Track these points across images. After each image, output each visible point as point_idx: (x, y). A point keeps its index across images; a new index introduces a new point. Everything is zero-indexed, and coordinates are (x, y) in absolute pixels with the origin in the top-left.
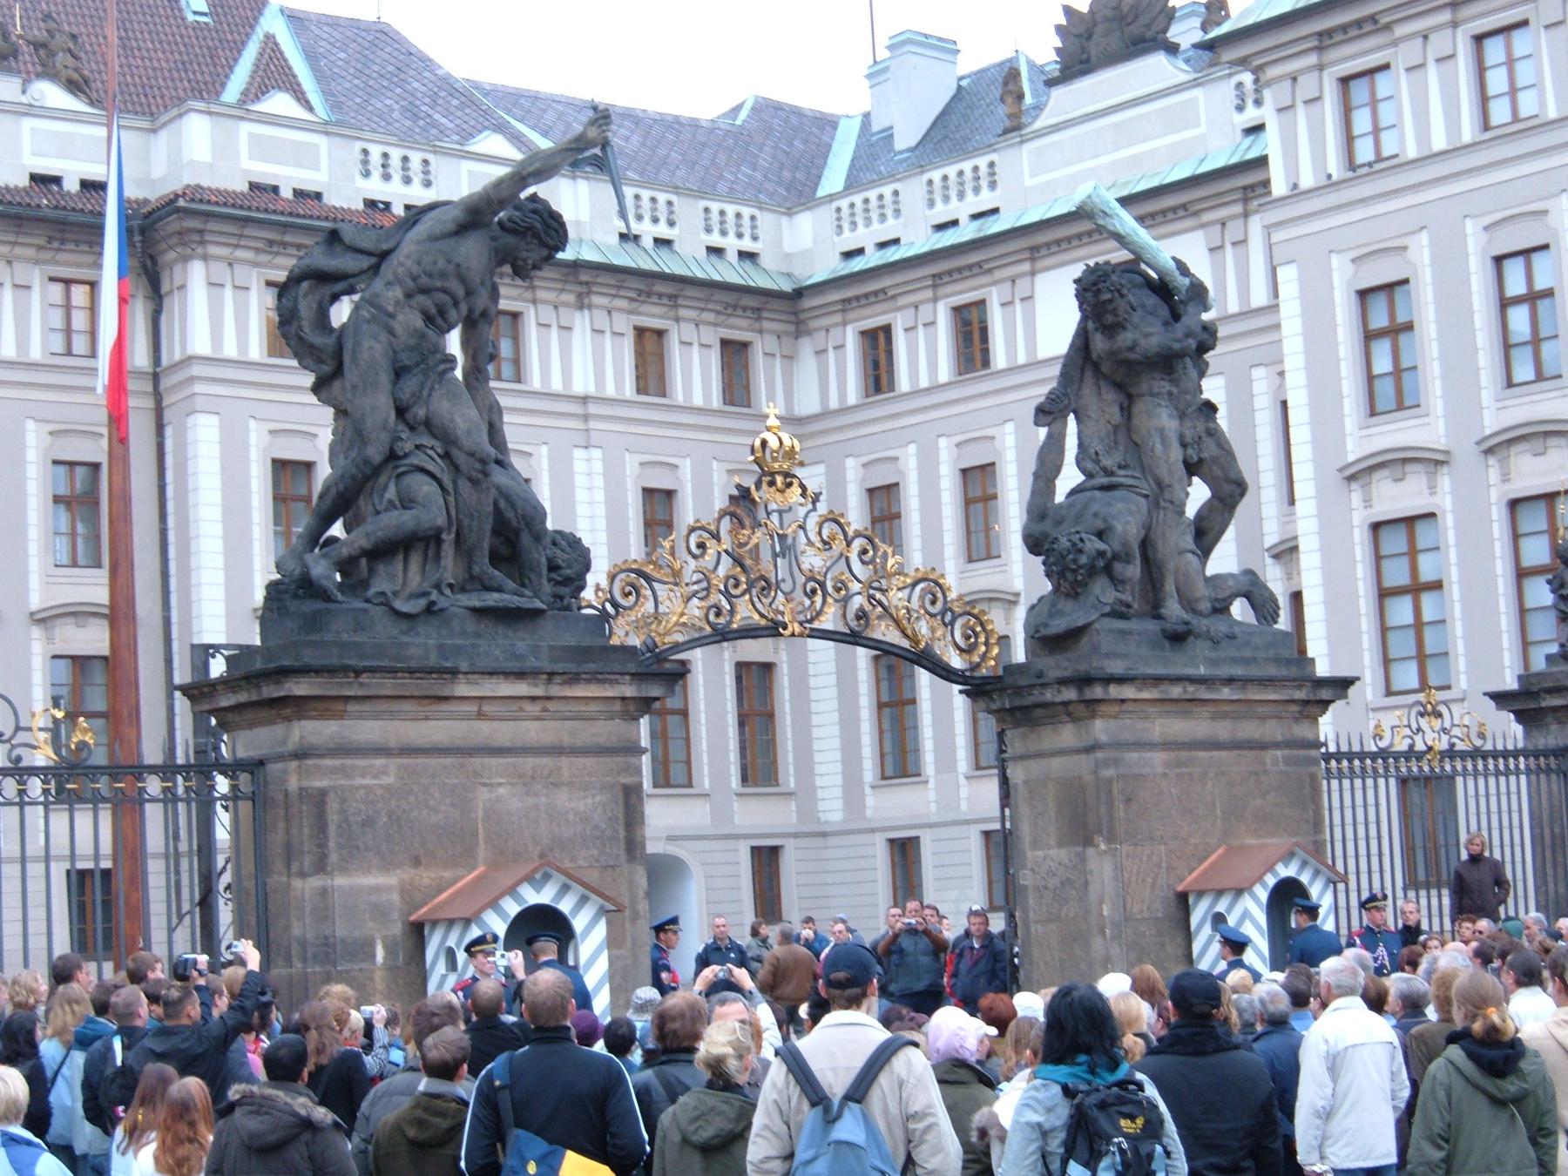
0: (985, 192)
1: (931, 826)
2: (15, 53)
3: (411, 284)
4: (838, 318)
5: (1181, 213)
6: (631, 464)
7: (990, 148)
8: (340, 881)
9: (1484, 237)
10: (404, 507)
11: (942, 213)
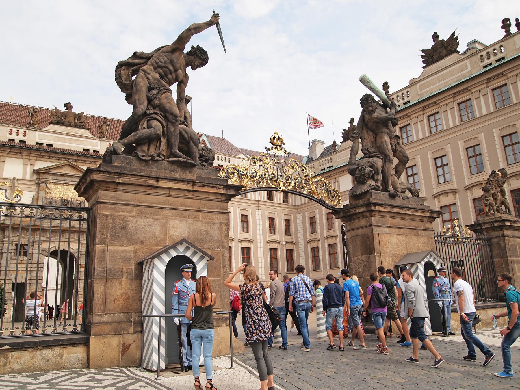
0: (330, 163)
1: (322, 279)
3: (156, 65)
7: (331, 155)
8: (110, 247)
9: (432, 155)
10: (148, 129)
11: (322, 167)
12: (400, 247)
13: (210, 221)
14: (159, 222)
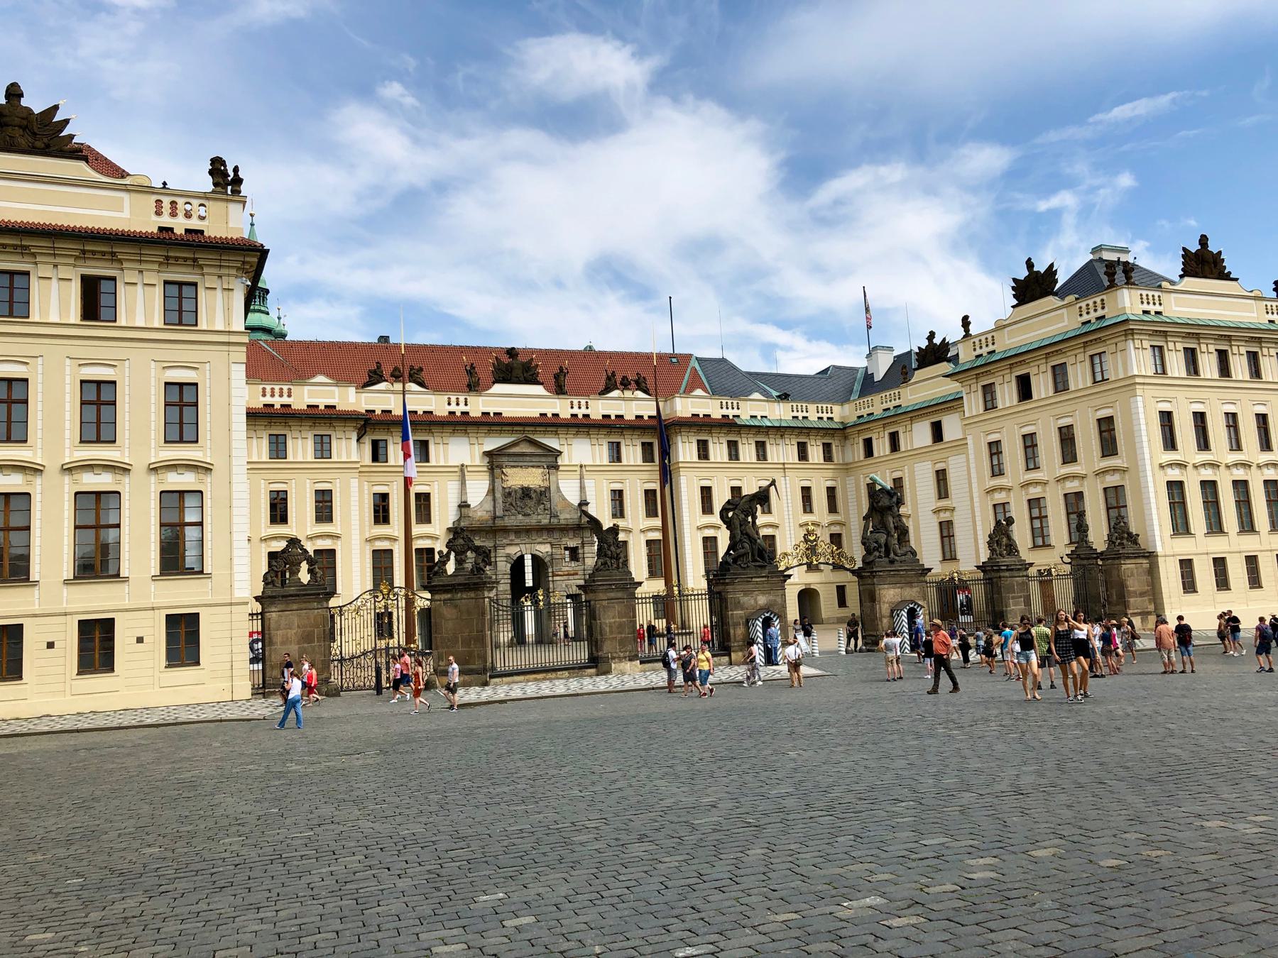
2: (630, 384)
11: (885, 406)
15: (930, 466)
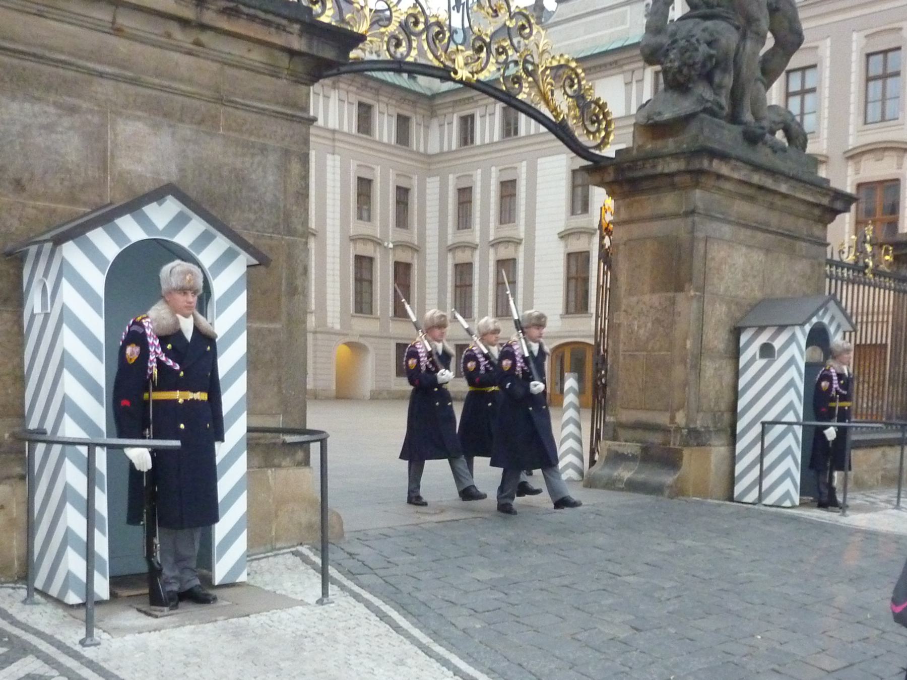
4: (450, 110)
5: (614, 66)
6: (353, 165)
12: (750, 279)
13: (252, 139)
14: (77, 120)
15: (564, 163)
